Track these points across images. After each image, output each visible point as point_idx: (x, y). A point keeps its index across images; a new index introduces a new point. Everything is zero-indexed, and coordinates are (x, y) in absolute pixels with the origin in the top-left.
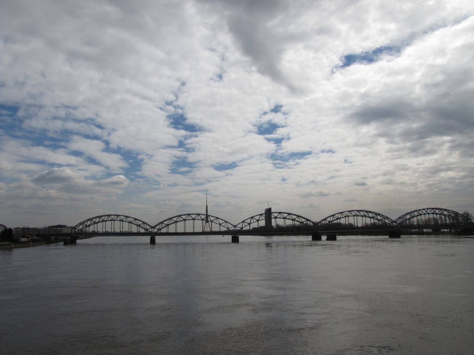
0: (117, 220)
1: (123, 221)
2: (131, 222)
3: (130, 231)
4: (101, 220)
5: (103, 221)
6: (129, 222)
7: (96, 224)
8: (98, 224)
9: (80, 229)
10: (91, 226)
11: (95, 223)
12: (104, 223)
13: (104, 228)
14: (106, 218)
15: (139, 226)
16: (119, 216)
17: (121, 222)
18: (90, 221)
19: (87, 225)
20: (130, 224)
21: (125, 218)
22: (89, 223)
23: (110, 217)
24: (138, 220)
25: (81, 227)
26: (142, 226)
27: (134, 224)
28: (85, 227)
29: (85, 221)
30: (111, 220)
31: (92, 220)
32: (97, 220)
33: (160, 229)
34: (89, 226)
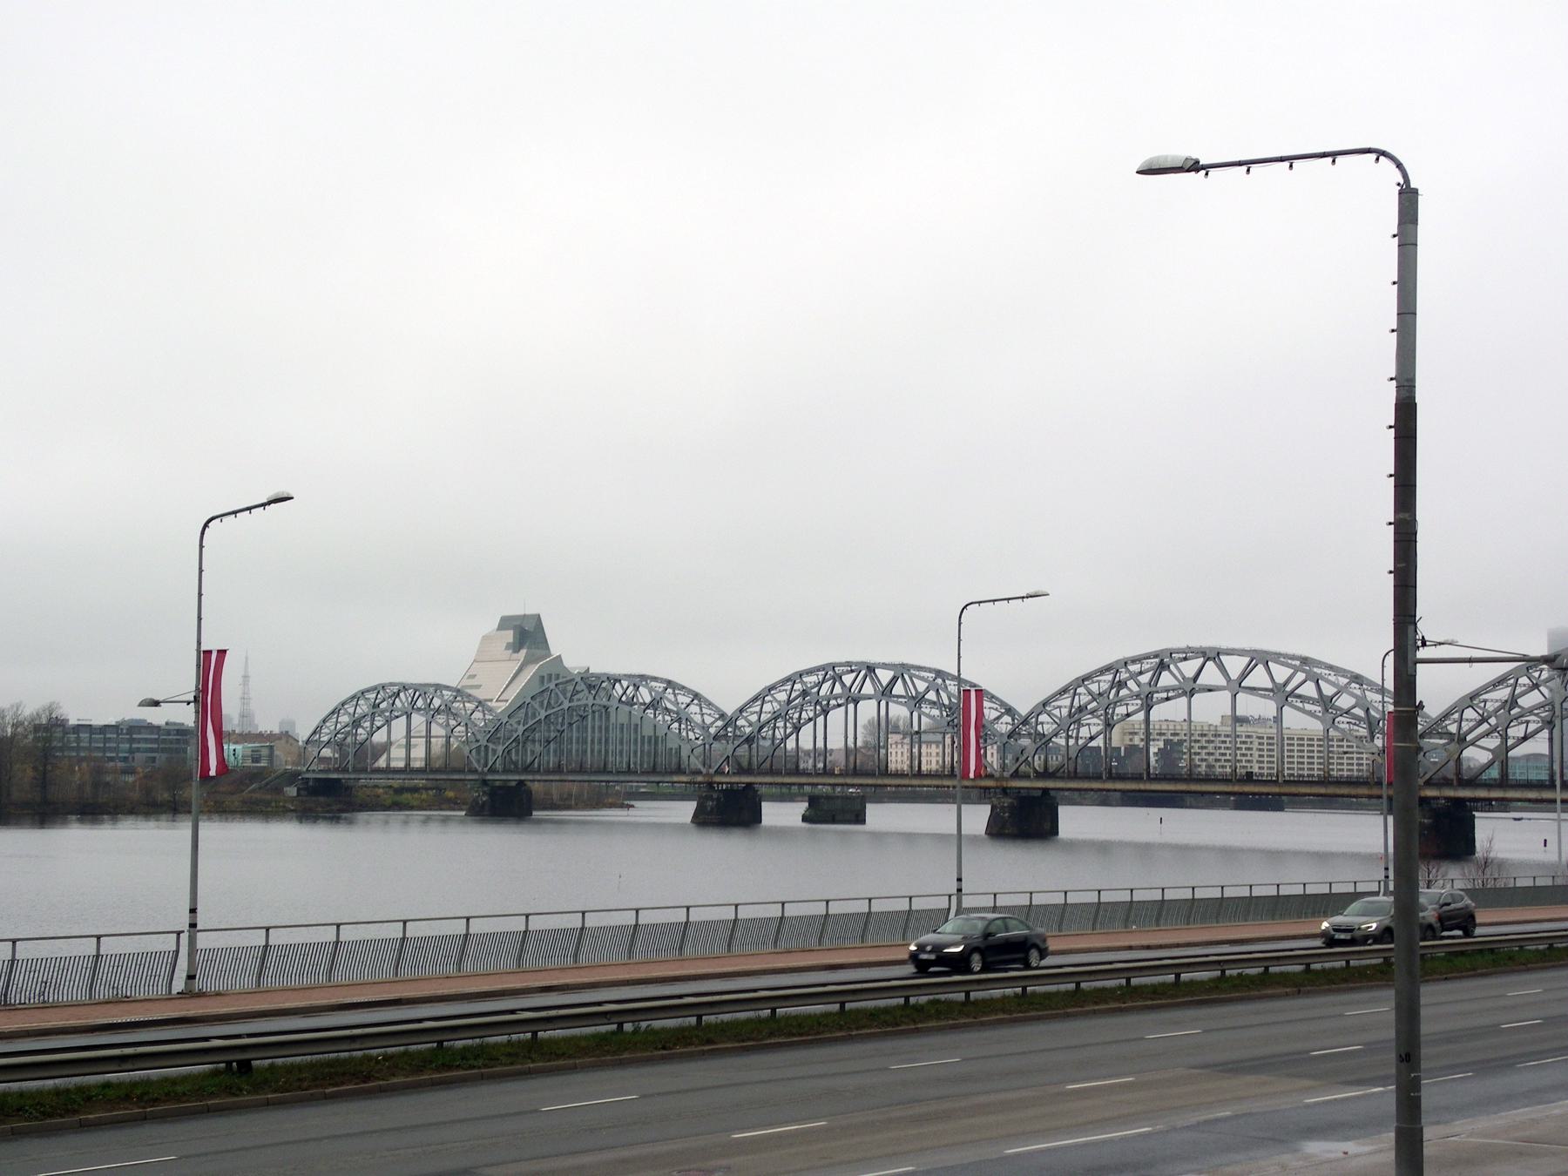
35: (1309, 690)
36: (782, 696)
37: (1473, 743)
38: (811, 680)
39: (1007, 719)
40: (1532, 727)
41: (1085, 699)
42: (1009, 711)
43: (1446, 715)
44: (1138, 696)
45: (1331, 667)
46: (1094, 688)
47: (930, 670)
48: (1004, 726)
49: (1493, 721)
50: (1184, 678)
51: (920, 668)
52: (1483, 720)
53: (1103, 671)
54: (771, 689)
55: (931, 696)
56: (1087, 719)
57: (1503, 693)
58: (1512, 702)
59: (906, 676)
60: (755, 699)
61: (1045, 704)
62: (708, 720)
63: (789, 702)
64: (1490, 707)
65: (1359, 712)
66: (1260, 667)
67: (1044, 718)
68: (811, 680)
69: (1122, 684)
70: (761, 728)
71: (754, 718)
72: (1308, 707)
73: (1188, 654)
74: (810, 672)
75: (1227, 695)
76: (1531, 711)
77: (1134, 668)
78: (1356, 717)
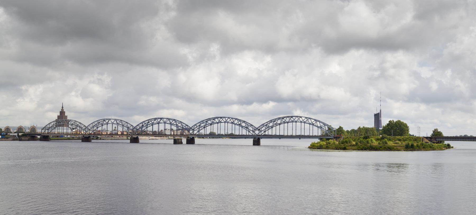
0: (298, 122)
1: (305, 122)
2: (313, 124)
3: (205, 134)
4: (283, 122)
5: (284, 123)
6: (310, 124)
7: (279, 126)
8: (281, 125)
9: (263, 131)
10: (273, 128)
11: (276, 125)
12: (286, 124)
13: (311, 131)
14: (288, 120)
15: (321, 127)
16: (301, 117)
17: (303, 124)
18: (273, 123)
19: (270, 126)
20: (311, 126)
21: (306, 119)
22: (271, 124)
23: (292, 118)
24: (320, 122)
25: (263, 128)
26: (323, 128)
27: (315, 126)
28: (267, 129)
29: (267, 123)
30: (292, 122)
31: (275, 121)
32: (279, 122)
33: (265, 132)
34: (272, 127)
35: (175, 123)
36: (53, 124)
37: (195, 130)
38: (100, 121)
39: (132, 127)
40: (202, 128)
41: (143, 124)
42: (132, 126)
43: (192, 127)
44: (151, 124)
45: (178, 121)
46: (145, 123)
47: (120, 120)
48: (131, 128)
49: (198, 127)
50: (158, 122)
51: (118, 120)
52: (197, 127)
53: (147, 121)
54: (51, 122)
55: (74, 124)
56: (95, 127)
57: (199, 124)
58: (200, 125)
59: (71, 122)
60: (49, 124)
61: (89, 125)
62: (82, 127)
63: (54, 124)
64: (198, 126)
65: (181, 126)
66: (110, 120)
67: (89, 127)
68: (100, 121)
69: (149, 122)
70: (49, 128)
71: (91, 126)
72: (175, 125)
73: (159, 118)
74: (100, 120)
75: (111, 124)
76: (202, 126)
77: (151, 120)
78: (181, 127)
